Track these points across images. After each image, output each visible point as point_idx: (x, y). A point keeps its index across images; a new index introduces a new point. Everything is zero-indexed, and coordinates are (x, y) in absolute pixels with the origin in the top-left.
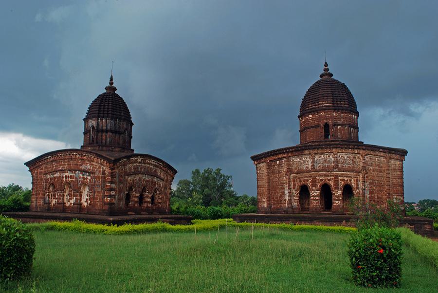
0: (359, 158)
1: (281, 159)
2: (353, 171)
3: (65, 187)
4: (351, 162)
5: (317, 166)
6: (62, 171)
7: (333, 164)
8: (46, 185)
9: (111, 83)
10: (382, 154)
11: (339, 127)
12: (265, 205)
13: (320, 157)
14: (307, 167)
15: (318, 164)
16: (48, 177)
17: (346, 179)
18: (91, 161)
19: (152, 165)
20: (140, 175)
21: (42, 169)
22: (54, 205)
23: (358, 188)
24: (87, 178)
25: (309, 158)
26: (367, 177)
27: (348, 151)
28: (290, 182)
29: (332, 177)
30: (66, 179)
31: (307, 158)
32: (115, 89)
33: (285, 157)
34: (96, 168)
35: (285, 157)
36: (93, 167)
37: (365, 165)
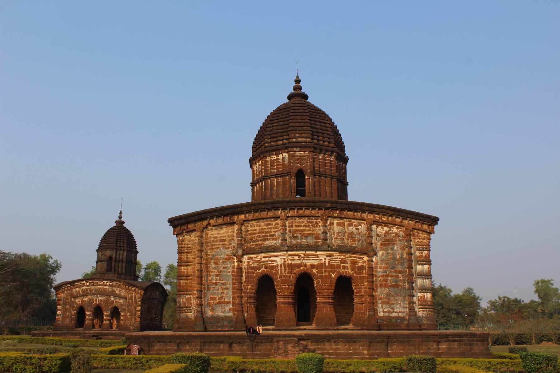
9: (120, 217)
19: (106, 285)
20: (89, 297)
32: (124, 223)
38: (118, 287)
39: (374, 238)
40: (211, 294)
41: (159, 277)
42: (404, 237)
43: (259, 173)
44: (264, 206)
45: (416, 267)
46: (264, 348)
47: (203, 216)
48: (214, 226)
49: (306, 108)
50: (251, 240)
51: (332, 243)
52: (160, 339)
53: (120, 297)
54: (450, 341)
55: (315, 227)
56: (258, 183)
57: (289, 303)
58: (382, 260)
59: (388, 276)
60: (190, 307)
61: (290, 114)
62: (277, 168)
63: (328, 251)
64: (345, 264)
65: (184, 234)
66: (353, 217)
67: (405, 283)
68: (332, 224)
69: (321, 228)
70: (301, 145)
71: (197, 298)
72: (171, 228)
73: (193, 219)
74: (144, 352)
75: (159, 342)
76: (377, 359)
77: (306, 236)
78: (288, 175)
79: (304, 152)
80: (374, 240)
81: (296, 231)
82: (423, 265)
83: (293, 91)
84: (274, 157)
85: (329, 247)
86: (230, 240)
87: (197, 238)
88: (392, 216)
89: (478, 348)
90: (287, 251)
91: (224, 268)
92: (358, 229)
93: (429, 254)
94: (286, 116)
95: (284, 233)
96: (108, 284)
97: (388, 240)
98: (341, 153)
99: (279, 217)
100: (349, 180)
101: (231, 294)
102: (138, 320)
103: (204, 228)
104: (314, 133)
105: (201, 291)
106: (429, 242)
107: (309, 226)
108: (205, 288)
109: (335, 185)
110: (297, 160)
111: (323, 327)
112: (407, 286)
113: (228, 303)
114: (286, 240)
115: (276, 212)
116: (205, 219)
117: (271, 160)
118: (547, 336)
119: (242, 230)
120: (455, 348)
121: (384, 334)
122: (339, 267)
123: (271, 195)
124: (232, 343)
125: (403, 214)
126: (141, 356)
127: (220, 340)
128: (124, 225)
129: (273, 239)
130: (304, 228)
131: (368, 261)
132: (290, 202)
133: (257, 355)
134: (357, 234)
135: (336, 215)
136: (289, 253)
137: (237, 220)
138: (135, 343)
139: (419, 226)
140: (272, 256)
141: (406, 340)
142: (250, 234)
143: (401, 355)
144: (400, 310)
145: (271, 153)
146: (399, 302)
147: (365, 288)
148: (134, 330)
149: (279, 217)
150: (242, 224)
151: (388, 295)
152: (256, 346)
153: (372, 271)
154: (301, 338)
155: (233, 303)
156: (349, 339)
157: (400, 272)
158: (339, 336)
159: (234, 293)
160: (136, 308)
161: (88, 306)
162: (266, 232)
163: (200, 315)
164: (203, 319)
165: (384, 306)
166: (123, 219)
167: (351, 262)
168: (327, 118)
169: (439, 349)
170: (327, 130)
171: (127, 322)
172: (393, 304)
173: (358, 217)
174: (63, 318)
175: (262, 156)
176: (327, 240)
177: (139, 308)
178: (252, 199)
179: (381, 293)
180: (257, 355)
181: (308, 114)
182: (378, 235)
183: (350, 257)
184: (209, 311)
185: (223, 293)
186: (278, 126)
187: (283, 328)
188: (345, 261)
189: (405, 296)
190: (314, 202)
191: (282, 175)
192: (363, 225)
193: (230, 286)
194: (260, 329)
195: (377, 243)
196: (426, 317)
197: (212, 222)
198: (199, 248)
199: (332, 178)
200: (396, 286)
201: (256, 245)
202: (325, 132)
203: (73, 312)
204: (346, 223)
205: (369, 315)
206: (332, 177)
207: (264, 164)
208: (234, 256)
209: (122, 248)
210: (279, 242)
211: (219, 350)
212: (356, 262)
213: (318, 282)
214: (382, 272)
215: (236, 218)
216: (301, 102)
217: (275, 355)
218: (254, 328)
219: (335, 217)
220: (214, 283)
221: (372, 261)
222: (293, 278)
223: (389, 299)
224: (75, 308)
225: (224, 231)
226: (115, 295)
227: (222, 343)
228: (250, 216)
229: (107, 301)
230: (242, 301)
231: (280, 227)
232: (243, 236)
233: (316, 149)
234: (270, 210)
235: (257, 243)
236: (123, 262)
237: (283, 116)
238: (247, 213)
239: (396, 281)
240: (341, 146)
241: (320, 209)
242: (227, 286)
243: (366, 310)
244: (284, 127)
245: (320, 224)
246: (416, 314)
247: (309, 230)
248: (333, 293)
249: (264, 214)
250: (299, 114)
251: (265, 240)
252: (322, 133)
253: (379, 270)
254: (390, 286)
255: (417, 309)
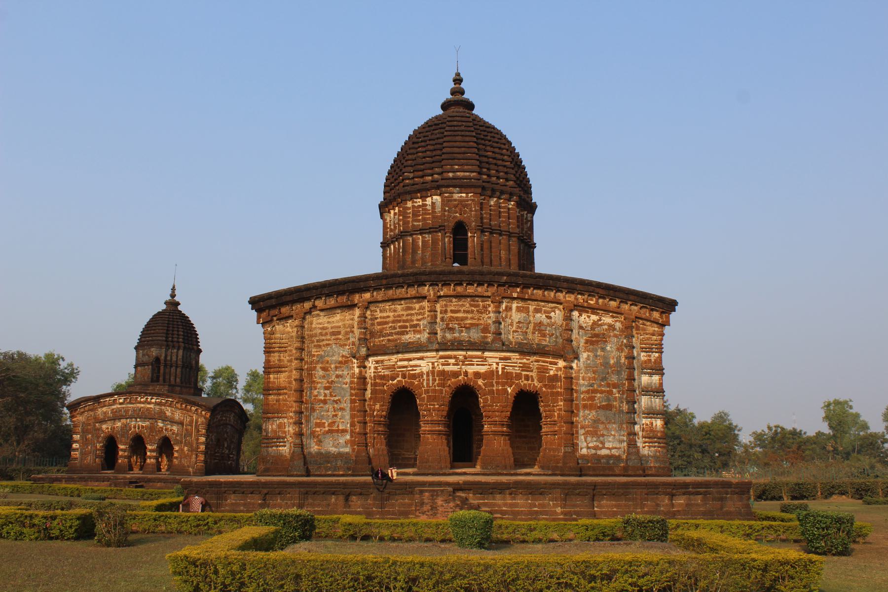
9: (173, 296)
19: (150, 403)
20: (124, 421)
32: (178, 304)
38: (170, 406)
39: (575, 331)
40: (317, 418)
41: (234, 391)
42: (622, 331)
43: (395, 227)
44: (401, 280)
45: (640, 379)
46: (400, 502)
47: (305, 295)
48: (322, 310)
49: (471, 124)
50: (381, 334)
51: (509, 339)
52: (236, 488)
53: (173, 422)
54: (690, 493)
55: (482, 313)
56: (393, 242)
57: (439, 433)
58: (587, 367)
59: (595, 391)
60: (283, 438)
61: (446, 133)
62: (424, 219)
63: (503, 351)
64: (528, 372)
65: (274, 323)
66: (543, 298)
67: (622, 402)
68: (509, 309)
69: (492, 315)
70: (461, 181)
71: (295, 423)
72: (254, 313)
73: (288, 298)
74: (210, 507)
75: (234, 493)
76: (576, 520)
77: (468, 328)
78: (440, 231)
79: (467, 193)
80: (574, 336)
81: (452, 319)
82: (651, 374)
83: (450, 96)
84: (419, 202)
85: (503, 345)
86: (347, 333)
87: (295, 329)
88: (604, 298)
89: (733, 504)
90: (437, 351)
91: (338, 376)
92: (550, 318)
93: (660, 358)
94: (438, 136)
95: (433, 323)
96: (153, 401)
97: (596, 335)
98: (525, 196)
99: (425, 298)
100: (536, 240)
101: (348, 417)
102: (202, 457)
103: (306, 313)
104: (484, 165)
105: (302, 413)
106: (662, 340)
107: (472, 312)
108: (306, 408)
109: (514, 248)
110: (456, 206)
111: (493, 471)
112: (625, 407)
113: (344, 431)
114: (436, 334)
115: (420, 289)
116: (308, 299)
117: (413, 206)
118: (839, 486)
119: (366, 318)
120: (698, 505)
121: (588, 483)
122: (519, 376)
123: (414, 262)
124: (349, 495)
125: (621, 295)
126: (205, 514)
127: (330, 489)
128: (180, 308)
129: (415, 332)
130: (465, 315)
131: (565, 367)
132: (442, 273)
133: (388, 513)
134: (548, 325)
135: (515, 295)
136: (441, 353)
137: (359, 302)
138: (197, 493)
139: (645, 313)
140: (414, 359)
141: (621, 491)
142: (379, 324)
143: (614, 514)
144: (613, 444)
145: (413, 195)
146: (613, 433)
147: (560, 410)
148: (195, 474)
149: (425, 298)
150: (367, 308)
151: (596, 421)
152: (388, 499)
153: (572, 384)
154: (457, 488)
155: (352, 431)
156: (533, 490)
157: (615, 386)
158: (517, 484)
159: (352, 417)
160: (198, 439)
161: (123, 436)
162: (404, 321)
163: (298, 450)
164: (305, 457)
165: (589, 439)
166: (177, 299)
167: (537, 368)
168: (503, 141)
169: (673, 505)
170: (503, 160)
171: (185, 462)
172: (603, 435)
173: (550, 299)
174: (81, 453)
175: (399, 200)
176: (500, 334)
177: (203, 439)
178: (383, 268)
179: (585, 417)
180: (388, 513)
181: (474, 134)
182: (581, 327)
183: (537, 361)
184: (313, 445)
185: (336, 415)
186: (426, 151)
187: (430, 472)
188: (529, 367)
189: (622, 424)
190: (481, 274)
191: (431, 230)
192: (557, 312)
193: (347, 405)
194: (393, 473)
195: (579, 339)
196: (654, 456)
197: (319, 303)
198: (298, 345)
199: (509, 236)
200: (608, 407)
201: (389, 340)
202: (500, 162)
203: (98, 446)
204: (531, 308)
205: (565, 452)
206: (510, 235)
207: (403, 213)
208: (354, 357)
209: (176, 344)
210: (424, 337)
211: (329, 505)
212: (546, 370)
213: (486, 400)
214: (587, 386)
215: (356, 298)
216: (462, 114)
217: (417, 513)
218: (385, 471)
219: (515, 299)
220: (321, 401)
221: (571, 368)
222: (446, 393)
223: (597, 427)
224: (100, 439)
225: (338, 319)
226: (165, 419)
227: (333, 494)
228: (379, 295)
229: (152, 428)
230: (365, 428)
231: (427, 313)
232: (368, 325)
233: (486, 190)
234: (410, 285)
235: (390, 338)
236: (177, 367)
237: (434, 137)
238: (375, 289)
239: (608, 399)
240: (525, 185)
241: (490, 284)
242: (342, 406)
243: (559, 445)
244: (434, 153)
245: (490, 309)
246: (638, 451)
247: (472, 318)
248: (509, 418)
249: (401, 292)
250: (459, 133)
251: (402, 333)
252: (496, 164)
253: (581, 382)
254: (599, 408)
255: (640, 444)
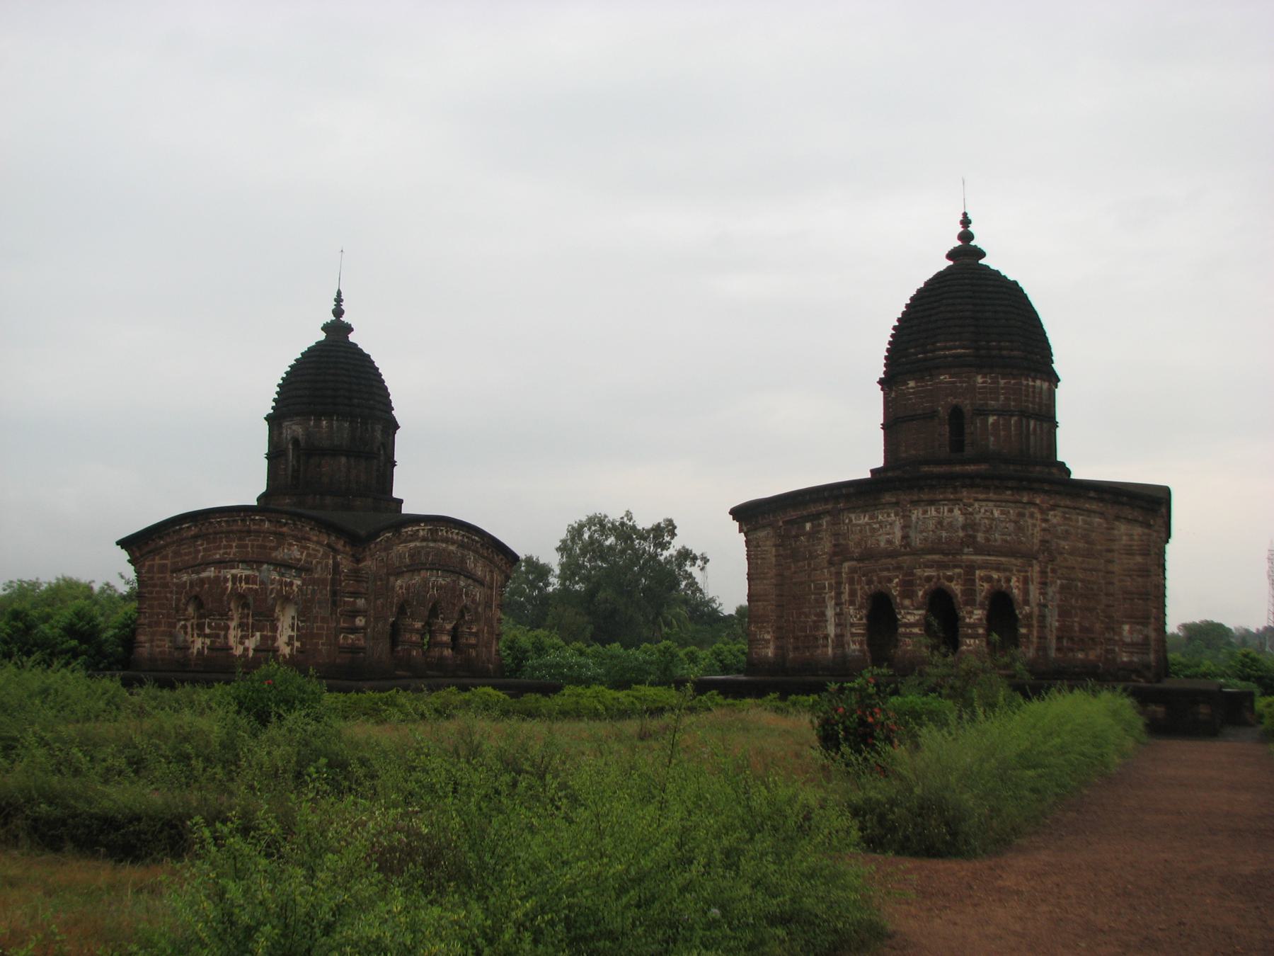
0: (1032, 515)
1: (818, 516)
2: (1013, 553)
3: (232, 605)
4: (1011, 526)
5: (916, 539)
6: (222, 564)
7: (961, 534)
8: (178, 600)
9: (338, 312)
10: (1094, 506)
11: (991, 420)
12: (770, 652)
13: (925, 512)
14: (889, 542)
15: (921, 532)
16: (185, 577)
17: (995, 576)
18: (302, 539)
19: (453, 542)
21: (165, 557)
22: (200, 652)
23: (1026, 602)
24: (291, 584)
25: (896, 515)
26: (1053, 571)
27: (1003, 497)
28: (839, 584)
29: (957, 570)
30: (234, 583)
31: (889, 515)
33: (828, 512)
34: (315, 557)
35: (828, 512)
36: (309, 555)
37: (1048, 537)
166: (344, 318)
226: (470, 576)
